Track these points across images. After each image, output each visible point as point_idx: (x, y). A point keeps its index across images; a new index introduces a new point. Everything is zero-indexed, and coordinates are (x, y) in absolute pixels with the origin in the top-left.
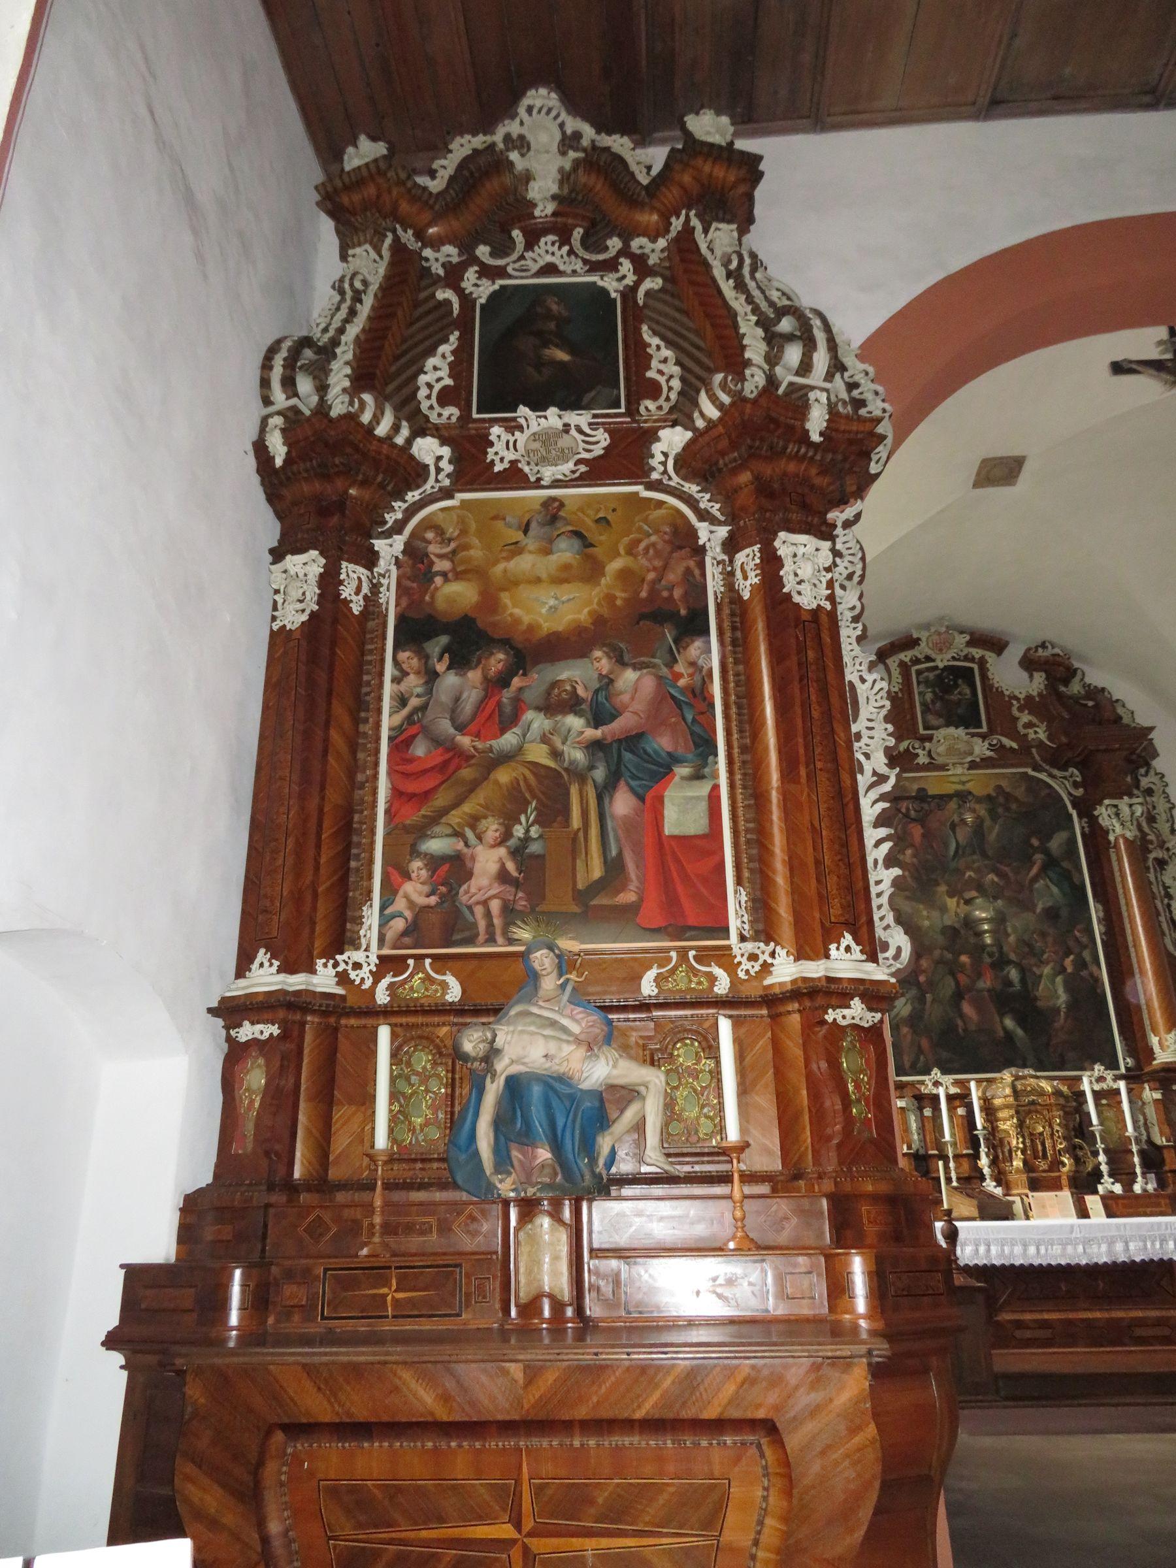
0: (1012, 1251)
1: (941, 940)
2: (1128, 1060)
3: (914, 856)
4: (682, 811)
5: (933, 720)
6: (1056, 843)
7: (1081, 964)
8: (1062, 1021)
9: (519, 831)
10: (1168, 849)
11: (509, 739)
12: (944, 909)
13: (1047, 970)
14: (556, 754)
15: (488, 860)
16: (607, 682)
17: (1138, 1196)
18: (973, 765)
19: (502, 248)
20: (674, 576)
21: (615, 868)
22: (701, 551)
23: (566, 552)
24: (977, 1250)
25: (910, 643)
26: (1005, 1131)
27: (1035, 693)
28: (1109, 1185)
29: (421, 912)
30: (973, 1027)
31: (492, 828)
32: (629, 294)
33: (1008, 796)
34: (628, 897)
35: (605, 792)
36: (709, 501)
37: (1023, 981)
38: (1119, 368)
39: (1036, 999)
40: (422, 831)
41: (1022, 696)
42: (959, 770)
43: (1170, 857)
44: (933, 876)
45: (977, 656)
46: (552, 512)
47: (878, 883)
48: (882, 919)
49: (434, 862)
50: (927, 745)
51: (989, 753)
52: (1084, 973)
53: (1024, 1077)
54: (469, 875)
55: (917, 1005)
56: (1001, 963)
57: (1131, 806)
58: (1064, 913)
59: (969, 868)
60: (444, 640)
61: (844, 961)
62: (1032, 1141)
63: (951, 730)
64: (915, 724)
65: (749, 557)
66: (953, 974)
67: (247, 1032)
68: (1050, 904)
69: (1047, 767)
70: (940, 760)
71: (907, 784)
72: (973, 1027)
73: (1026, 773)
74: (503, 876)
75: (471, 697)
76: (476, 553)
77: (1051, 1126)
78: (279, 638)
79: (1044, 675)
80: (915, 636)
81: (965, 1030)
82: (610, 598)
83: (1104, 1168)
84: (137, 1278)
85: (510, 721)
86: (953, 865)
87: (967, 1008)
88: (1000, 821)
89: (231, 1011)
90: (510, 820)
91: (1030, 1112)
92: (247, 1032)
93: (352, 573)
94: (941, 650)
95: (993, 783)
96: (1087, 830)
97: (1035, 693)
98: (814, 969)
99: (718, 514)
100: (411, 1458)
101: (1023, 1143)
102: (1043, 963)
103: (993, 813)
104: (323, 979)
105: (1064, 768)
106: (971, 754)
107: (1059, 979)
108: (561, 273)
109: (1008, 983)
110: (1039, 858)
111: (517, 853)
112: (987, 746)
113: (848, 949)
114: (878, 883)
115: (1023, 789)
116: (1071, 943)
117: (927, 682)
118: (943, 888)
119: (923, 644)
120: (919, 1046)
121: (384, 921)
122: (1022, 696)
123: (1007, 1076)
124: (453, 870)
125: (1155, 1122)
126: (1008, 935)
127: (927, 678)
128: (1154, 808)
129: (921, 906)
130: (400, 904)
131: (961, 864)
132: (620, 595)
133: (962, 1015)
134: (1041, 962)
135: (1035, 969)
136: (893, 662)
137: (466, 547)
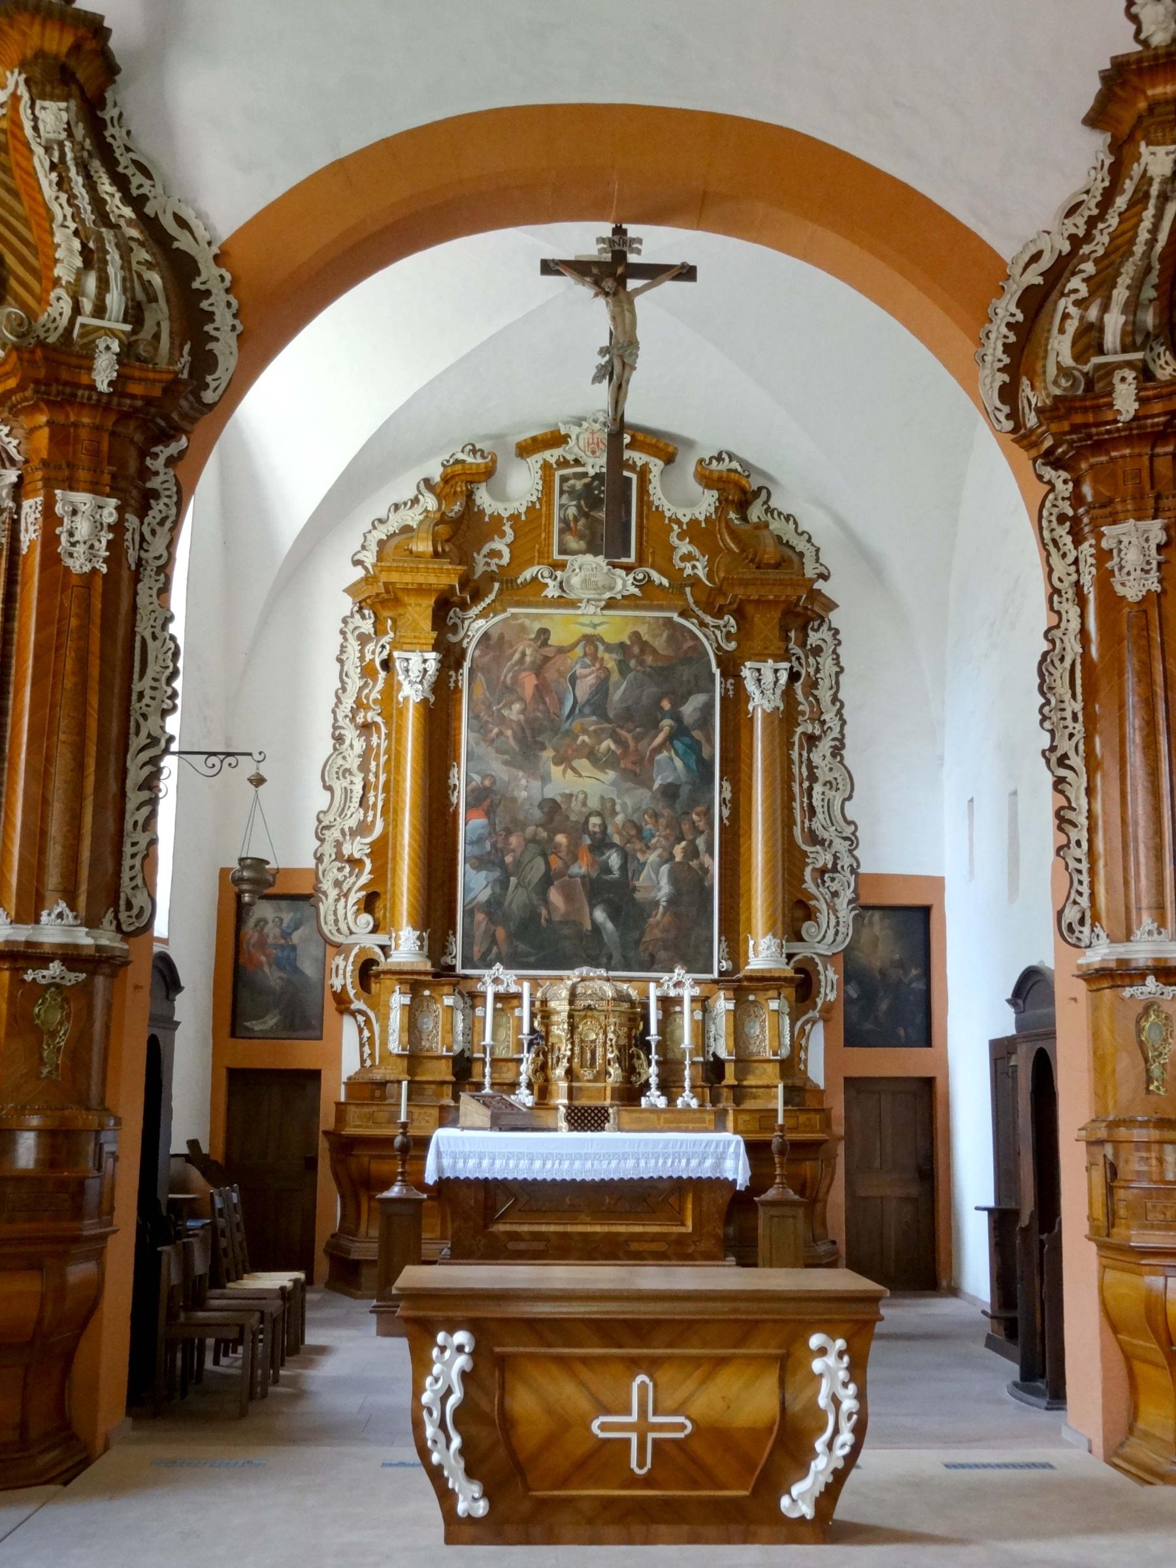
0: (517, 1165)
1: (537, 814)
2: (724, 963)
3: (523, 712)
5: (573, 543)
6: (690, 709)
7: (692, 852)
8: (659, 917)
10: (823, 723)
12: (545, 779)
13: (653, 857)
17: (680, 1111)
18: (611, 604)
24: (480, 1163)
25: (556, 439)
26: (559, 1037)
27: (702, 518)
28: (655, 1098)
30: (556, 918)
33: (644, 646)
36: (7, 435)
37: (624, 868)
38: (549, 267)
39: (635, 889)
41: (685, 520)
42: (591, 609)
43: (825, 732)
44: (539, 739)
45: (639, 463)
47: (134, 844)
48: (132, 879)
50: (559, 573)
51: (634, 590)
52: (694, 863)
53: (592, 979)
55: (498, 890)
56: (601, 844)
57: (776, 671)
58: (685, 791)
59: (585, 731)
61: (54, 928)
62: (582, 1048)
63: (589, 557)
64: (550, 545)
66: (544, 855)
68: (669, 780)
69: (700, 613)
70: (572, 596)
71: (527, 622)
72: (556, 918)
73: (670, 619)
77: (605, 1033)
79: (716, 494)
80: (563, 432)
81: (548, 921)
83: (653, 1081)
86: (567, 725)
87: (555, 896)
88: (631, 676)
91: (585, 1017)
94: (593, 452)
95: (630, 629)
96: (731, 693)
97: (702, 518)
99: (13, 452)
101: (572, 1050)
102: (648, 848)
105: (719, 614)
106: (611, 589)
107: (665, 869)
109: (609, 871)
110: (667, 724)
112: (631, 580)
113: (60, 915)
114: (134, 844)
115: (665, 636)
116: (685, 827)
117: (572, 492)
119: (572, 443)
120: (494, 936)
122: (685, 520)
123: (573, 975)
125: (723, 1034)
126: (617, 814)
127: (573, 486)
128: (818, 670)
129: (521, 774)
131: (576, 724)
133: (546, 902)
134: (648, 848)
135: (639, 855)
136: (535, 461)
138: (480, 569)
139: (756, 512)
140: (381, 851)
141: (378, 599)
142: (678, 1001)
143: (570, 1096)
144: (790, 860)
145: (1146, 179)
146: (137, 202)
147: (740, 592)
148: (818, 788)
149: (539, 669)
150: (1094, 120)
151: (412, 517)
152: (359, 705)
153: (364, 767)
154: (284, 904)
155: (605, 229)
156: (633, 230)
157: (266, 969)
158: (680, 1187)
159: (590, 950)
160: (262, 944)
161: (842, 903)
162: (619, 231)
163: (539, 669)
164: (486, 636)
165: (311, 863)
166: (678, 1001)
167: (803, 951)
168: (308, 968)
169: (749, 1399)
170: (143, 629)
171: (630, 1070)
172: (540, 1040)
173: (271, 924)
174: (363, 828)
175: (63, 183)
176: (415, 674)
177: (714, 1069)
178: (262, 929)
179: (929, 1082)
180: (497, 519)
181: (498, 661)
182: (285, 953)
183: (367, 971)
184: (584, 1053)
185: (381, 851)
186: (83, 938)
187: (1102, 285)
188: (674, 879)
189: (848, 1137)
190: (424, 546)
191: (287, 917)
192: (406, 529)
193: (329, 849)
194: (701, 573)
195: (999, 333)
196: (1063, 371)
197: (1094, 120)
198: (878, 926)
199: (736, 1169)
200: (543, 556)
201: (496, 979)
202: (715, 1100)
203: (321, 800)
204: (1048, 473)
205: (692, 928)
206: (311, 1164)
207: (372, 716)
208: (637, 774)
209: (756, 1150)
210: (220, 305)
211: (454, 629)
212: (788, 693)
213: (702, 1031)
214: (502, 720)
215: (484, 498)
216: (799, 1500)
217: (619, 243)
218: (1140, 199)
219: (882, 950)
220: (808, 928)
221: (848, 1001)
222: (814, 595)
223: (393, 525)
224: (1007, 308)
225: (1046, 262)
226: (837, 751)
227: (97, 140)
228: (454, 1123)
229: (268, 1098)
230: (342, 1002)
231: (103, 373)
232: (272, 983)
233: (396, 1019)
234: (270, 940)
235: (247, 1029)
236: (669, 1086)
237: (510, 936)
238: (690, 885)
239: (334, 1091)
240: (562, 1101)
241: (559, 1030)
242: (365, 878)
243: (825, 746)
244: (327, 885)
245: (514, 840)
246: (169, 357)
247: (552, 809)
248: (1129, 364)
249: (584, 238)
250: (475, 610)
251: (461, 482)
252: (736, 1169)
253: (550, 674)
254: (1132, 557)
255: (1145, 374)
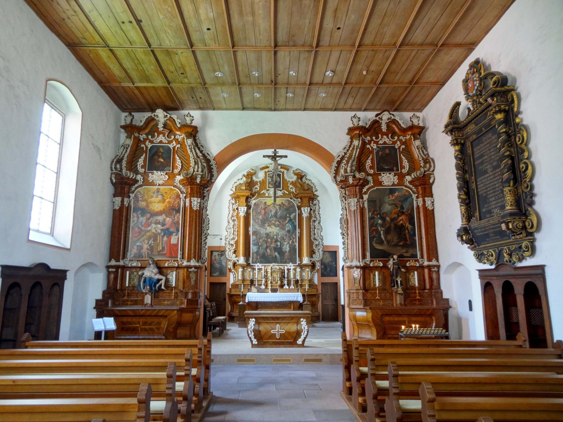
1: (265, 236)
4: (174, 240)
5: (271, 186)
6: (292, 216)
7: (293, 242)
9: (150, 242)
11: (149, 228)
12: (266, 229)
13: (286, 243)
14: (156, 231)
15: (146, 246)
16: (165, 220)
19: (153, 136)
20: (176, 203)
21: (163, 248)
22: (180, 199)
23: (160, 198)
25: (267, 167)
28: (286, 287)
29: (135, 254)
31: (146, 241)
32: (174, 148)
33: (284, 205)
34: (165, 252)
35: (163, 237)
37: (280, 245)
38: (264, 156)
40: (136, 242)
46: (158, 191)
49: (138, 246)
54: (143, 248)
56: (276, 241)
58: (291, 231)
60: (140, 212)
61: (193, 263)
65: (188, 200)
67: (111, 270)
74: (147, 249)
75: (144, 221)
76: (146, 197)
78: (114, 210)
82: (166, 206)
84: (97, 301)
85: (149, 225)
87: (268, 250)
89: (108, 267)
90: (149, 241)
92: (111, 270)
93: (126, 200)
98: (188, 264)
100: (129, 319)
102: (285, 241)
103: (280, 208)
104: (121, 263)
105: (297, 198)
108: (163, 143)
109: (278, 245)
111: (149, 246)
118: (267, 225)
121: (130, 255)
123: (272, 265)
124: (141, 248)
130: (133, 252)
131: (271, 219)
132: (168, 205)
136: (264, 171)
137: (144, 196)
138: (254, 191)
139: (304, 179)
140: (237, 243)
141: (236, 197)
142: (290, 269)
143: (271, 286)
144: (311, 243)
145: (354, 146)
146: (201, 152)
147: (301, 195)
148: (316, 230)
149: (265, 209)
150: (348, 134)
151: (242, 182)
152: (232, 216)
153: (233, 227)
155: (273, 150)
156: (277, 150)
158: (291, 302)
159: (275, 260)
160: (215, 260)
161: (320, 251)
162: (275, 150)
163: (265, 209)
164: (255, 203)
165: (224, 245)
166: (290, 269)
167: (313, 260)
168: (224, 264)
169: (293, 328)
170: (204, 217)
171: (282, 282)
172: (266, 277)
174: (233, 239)
175: (191, 151)
176: (242, 211)
177: (297, 282)
179: (337, 283)
180: (257, 182)
181: (257, 208)
183: (234, 264)
184: (274, 279)
185: (237, 243)
186: (197, 264)
187: (348, 162)
188: (290, 247)
189: (322, 293)
190: (244, 188)
192: (240, 184)
193: (227, 242)
194: (294, 191)
195: (333, 168)
196: (342, 175)
197: (348, 134)
198: (327, 254)
199: (300, 299)
200: (265, 188)
201: (258, 266)
202: (297, 287)
203: (226, 233)
204: (341, 190)
205: (293, 256)
206: (225, 299)
207: (235, 218)
208: (283, 227)
209: (303, 295)
210: (214, 167)
211: (249, 202)
212: (310, 213)
213: (295, 275)
214: (258, 219)
215: (254, 178)
216: (300, 342)
217: (275, 152)
218: (353, 148)
219: (328, 259)
220: (314, 256)
221: (322, 269)
222: (314, 195)
223: (238, 183)
224: (335, 164)
225: (341, 157)
226: (319, 223)
227: (197, 145)
228: (251, 292)
229: (217, 288)
230: (230, 270)
231: (198, 181)
233: (240, 273)
236: (289, 284)
237: (261, 258)
238: (293, 249)
239: (229, 286)
240: (270, 287)
241: (269, 275)
242: (234, 247)
243: (317, 222)
244: (227, 249)
245: (261, 240)
246: (207, 177)
247: (267, 235)
248: (351, 175)
249: (270, 152)
250: (253, 199)
251: (250, 175)
252: (300, 299)
253: (267, 210)
254: (352, 204)
255: (354, 176)
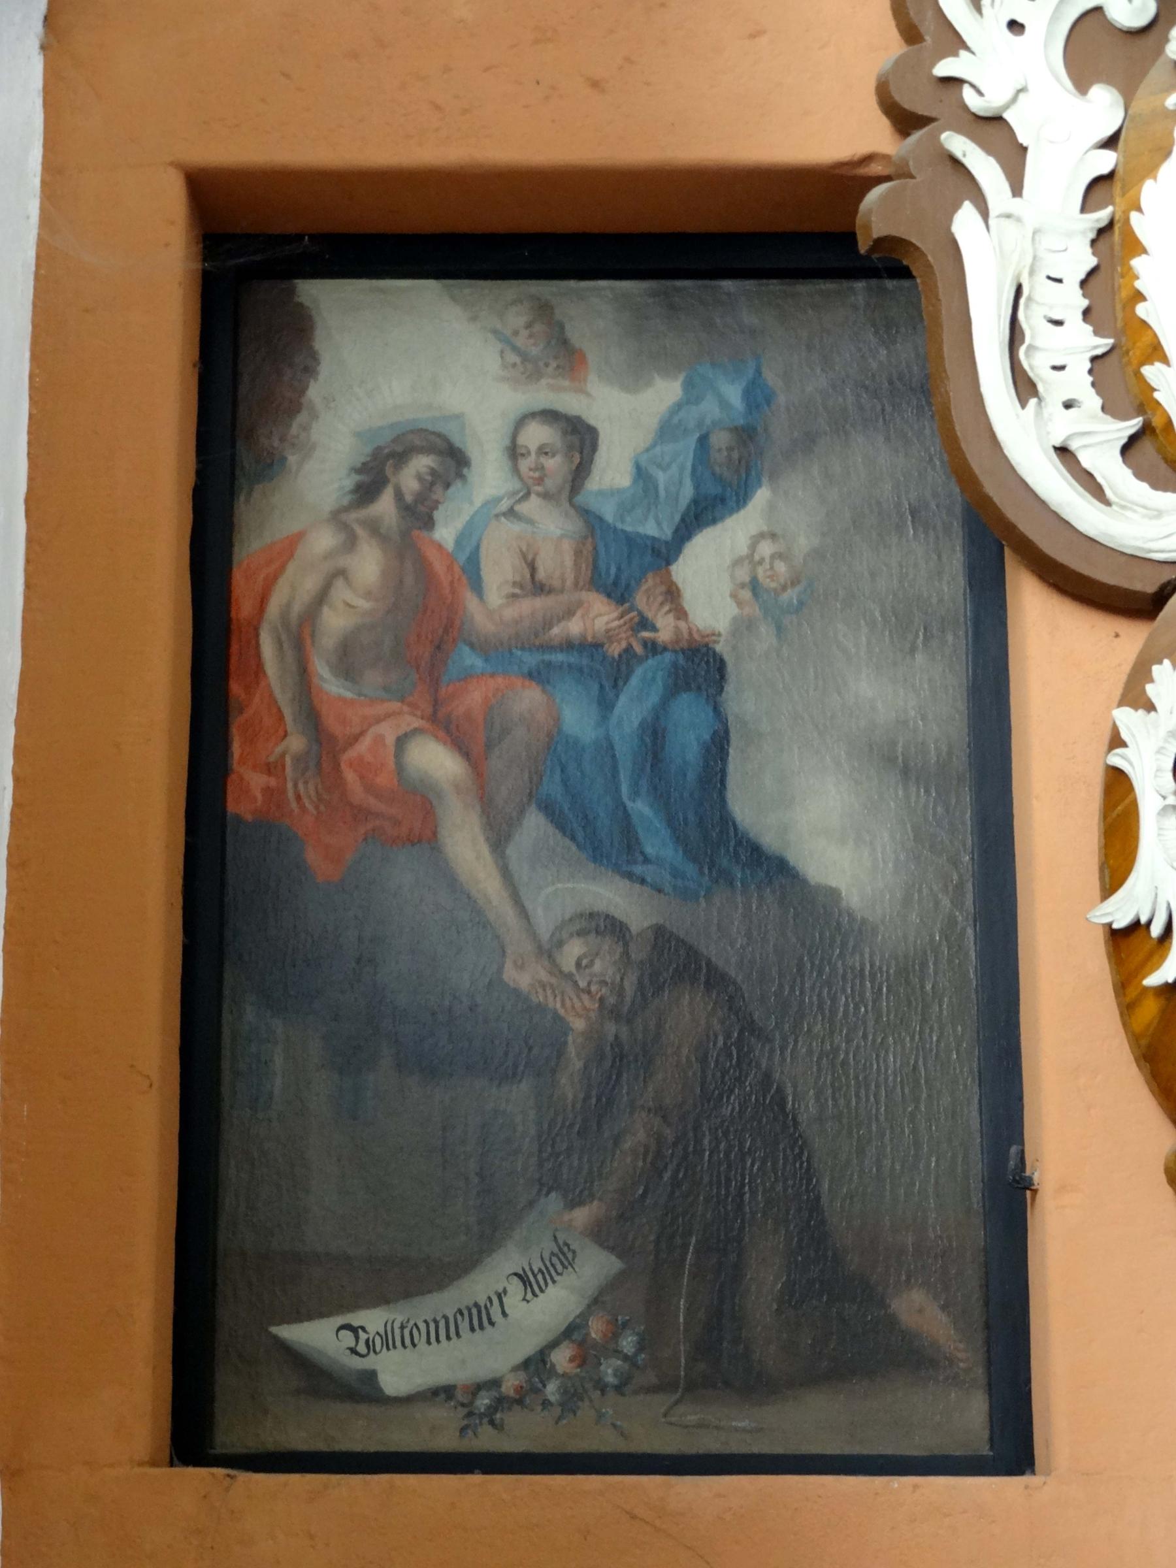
154: (594, 308)
157: (465, 844)
160: (424, 632)
168: (838, 832)
173: (490, 478)
178: (419, 514)
182: (631, 709)
191: (633, 413)
232: (523, 977)
234: (494, 605)
235: (315, 1379)
